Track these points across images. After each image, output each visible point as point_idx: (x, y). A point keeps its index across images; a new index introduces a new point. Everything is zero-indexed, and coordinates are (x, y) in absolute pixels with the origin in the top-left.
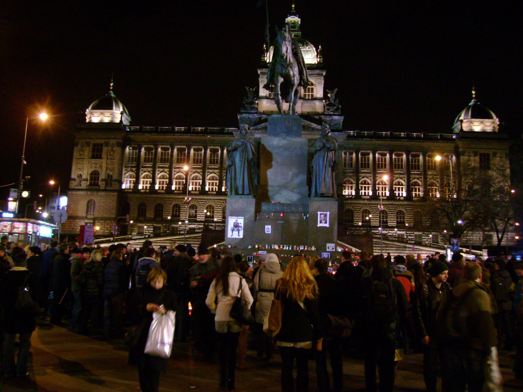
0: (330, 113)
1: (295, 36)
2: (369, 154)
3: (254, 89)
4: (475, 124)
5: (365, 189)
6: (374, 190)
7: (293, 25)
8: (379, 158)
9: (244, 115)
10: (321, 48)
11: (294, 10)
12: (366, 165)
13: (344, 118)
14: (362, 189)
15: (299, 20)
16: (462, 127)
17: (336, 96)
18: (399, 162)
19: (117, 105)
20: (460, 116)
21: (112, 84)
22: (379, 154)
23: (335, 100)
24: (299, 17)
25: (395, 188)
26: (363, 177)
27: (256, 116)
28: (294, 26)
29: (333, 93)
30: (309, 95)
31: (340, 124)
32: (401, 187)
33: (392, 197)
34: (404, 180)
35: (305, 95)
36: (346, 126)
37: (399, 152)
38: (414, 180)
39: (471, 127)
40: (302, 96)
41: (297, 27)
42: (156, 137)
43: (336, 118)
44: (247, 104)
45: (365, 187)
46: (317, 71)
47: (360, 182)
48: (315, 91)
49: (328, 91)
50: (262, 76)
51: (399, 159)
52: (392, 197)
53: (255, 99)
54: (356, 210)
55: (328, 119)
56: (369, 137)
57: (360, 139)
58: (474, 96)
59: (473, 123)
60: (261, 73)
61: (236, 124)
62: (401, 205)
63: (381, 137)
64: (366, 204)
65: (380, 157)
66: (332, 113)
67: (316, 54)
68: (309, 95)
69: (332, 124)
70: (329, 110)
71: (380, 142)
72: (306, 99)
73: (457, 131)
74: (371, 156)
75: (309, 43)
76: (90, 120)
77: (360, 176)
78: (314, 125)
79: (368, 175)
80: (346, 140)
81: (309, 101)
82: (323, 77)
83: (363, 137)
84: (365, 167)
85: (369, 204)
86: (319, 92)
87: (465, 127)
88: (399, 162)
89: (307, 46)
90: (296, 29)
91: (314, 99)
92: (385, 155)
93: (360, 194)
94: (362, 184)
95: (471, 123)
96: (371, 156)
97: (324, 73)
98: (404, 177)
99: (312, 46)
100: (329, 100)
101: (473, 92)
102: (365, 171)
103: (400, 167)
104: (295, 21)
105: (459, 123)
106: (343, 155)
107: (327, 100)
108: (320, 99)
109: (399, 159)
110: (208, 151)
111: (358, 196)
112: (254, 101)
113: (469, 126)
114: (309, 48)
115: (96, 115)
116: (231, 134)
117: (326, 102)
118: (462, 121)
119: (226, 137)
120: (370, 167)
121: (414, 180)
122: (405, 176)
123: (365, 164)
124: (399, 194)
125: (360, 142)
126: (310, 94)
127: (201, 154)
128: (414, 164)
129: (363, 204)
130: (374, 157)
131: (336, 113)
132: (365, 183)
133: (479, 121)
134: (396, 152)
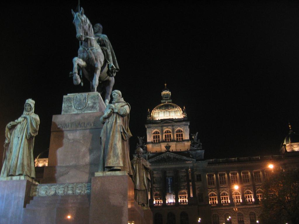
0: (194, 149)
1: (168, 102)
2: (225, 175)
3: (143, 138)
4: (295, 146)
5: (225, 199)
6: (231, 199)
7: (166, 96)
8: (231, 176)
10: (185, 108)
11: (166, 87)
12: (224, 182)
13: (205, 151)
14: (223, 199)
15: (170, 92)
16: (286, 149)
17: (197, 137)
18: (246, 177)
20: (284, 142)
22: (231, 174)
23: (197, 140)
24: (169, 91)
25: (246, 196)
26: (223, 191)
28: (167, 97)
29: (195, 135)
30: (180, 139)
31: (202, 155)
32: (250, 195)
33: (245, 203)
34: (251, 190)
35: (177, 139)
36: (206, 157)
37: (245, 171)
38: (259, 190)
39: (292, 148)
40: (176, 140)
41: (169, 97)
43: (199, 151)
45: (225, 198)
46: (184, 123)
47: (221, 194)
48: (183, 136)
49: (192, 135)
50: (148, 129)
51: (246, 176)
52: (245, 203)
53: (144, 144)
54: (220, 215)
55: (194, 152)
56: (224, 162)
57: (217, 164)
58: (290, 128)
59: (293, 146)
60: (147, 127)
62: (252, 208)
63: (232, 162)
64: (227, 209)
65: (233, 175)
66: (196, 149)
67: (182, 112)
68: (180, 139)
69: (197, 156)
70: (193, 147)
71: (231, 165)
72: (178, 141)
73: (284, 152)
74: (226, 175)
75: (178, 106)
76: (38, 165)
77: (221, 190)
78: (185, 158)
79: (225, 189)
80: (208, 166)
81: (180, 142)
82: (188, 126)
83: (219, 163)
84: (223, 183)
85: (229, 209)
86: (186, 136)
87: (288, 149)
88: (246, 177)
89: (176, 108)
90: (169, 98)
91: (183, 141)
93: (222, 203)
94: (222, 195)
95: (292, 146)
96: (226, 175)
97: (189, 124)
98: (251, 188)
99: (179, 107)
100: (193, 141)
101: (290, 126)
102: (224, 186)
104: (167, 94)
105: (283, 147)
106: (207, 176)
107: (192, 141)
108: (187, 141)
109: (246, 176)
111: (220, 205)
112: (143, 145)
113: (290, 148)
114: (177, 109)
115: (41, 162)
117: (191, 142)
118: (285, 145)
120: (227, 183)
121: (259, 190)
122: (252, 187)
123: (223, 181)
124: (249, 200)
125: (217, 166)
126: (181, 138)
128: (256, 178)
129: (225, 209)
130: (228, 176)
131: (199, 149)
132: (224, 194)
133: (296, 145)
134: (243, 171)
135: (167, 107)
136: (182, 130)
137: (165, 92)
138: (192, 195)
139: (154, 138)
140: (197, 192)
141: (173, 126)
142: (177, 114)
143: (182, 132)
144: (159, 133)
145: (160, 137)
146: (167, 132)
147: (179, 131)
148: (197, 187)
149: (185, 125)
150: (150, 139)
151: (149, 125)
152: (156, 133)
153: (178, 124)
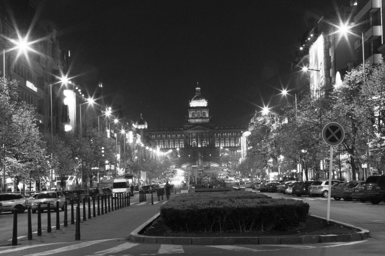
9: (185, 125)
12: (222, 137)
19: (145, 122)
21: (141, 115)
27: (189, 126)
42: (158, 132)
43: (212, 125)
44: (186, 122)
46: (206, 109)
61: (183, 127)
74: (224, 134)
78: (206, 128)
86: (207, 115)
91: (206, 118)
92: (228, 134)
96: (224, 134)
103: (232, 137)
108: (207, 118)
110: (175, 135)
116: (182, 130)
119: (180, 131)
127: (172, 136)
135: (198, 98)
136: (205, 112)
137: (198, 88)
138: (208, 143)
139: (192, 115)
140: (210, 142)
141: (201, 110)
142: (203, 103)
143: (205, 113)
144: (194, 113)
145: (195, 115)
146: (198, 113)
147: (204, 113)
148: (210, 140)
149: (207, 110)
150: (190, 116)
151: (190, 109)
152: (193, 113)
153: (203, 109)
